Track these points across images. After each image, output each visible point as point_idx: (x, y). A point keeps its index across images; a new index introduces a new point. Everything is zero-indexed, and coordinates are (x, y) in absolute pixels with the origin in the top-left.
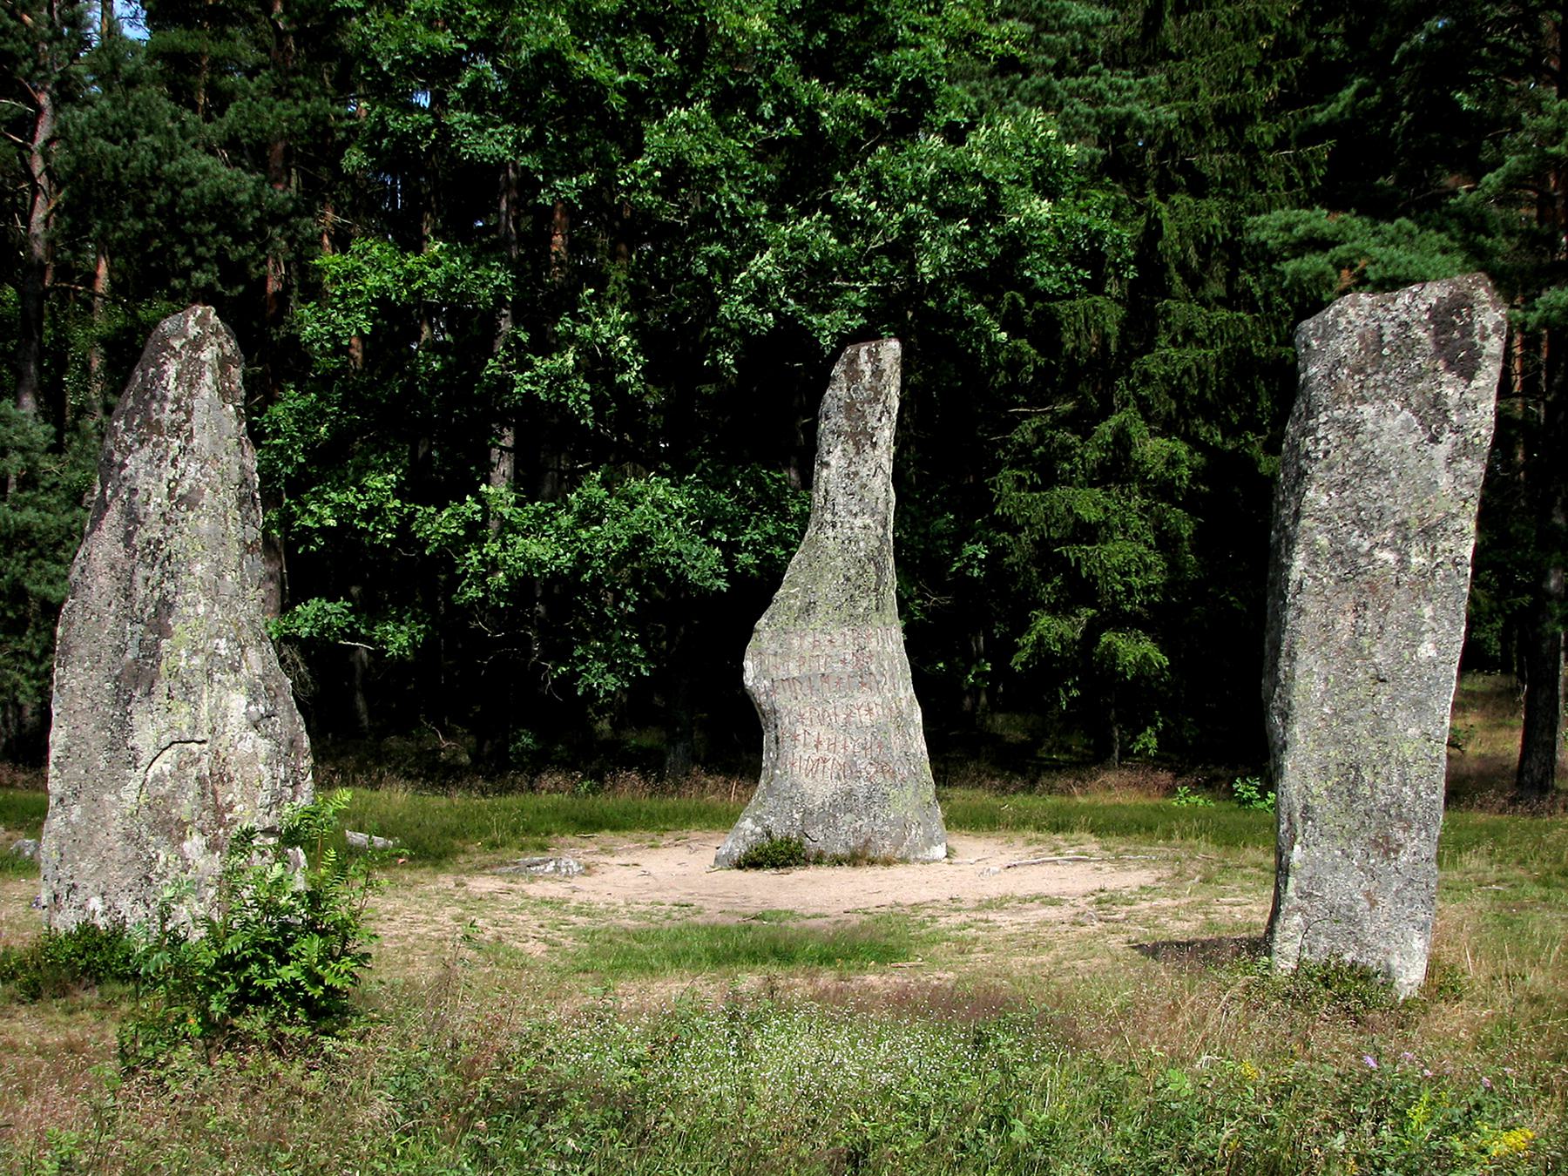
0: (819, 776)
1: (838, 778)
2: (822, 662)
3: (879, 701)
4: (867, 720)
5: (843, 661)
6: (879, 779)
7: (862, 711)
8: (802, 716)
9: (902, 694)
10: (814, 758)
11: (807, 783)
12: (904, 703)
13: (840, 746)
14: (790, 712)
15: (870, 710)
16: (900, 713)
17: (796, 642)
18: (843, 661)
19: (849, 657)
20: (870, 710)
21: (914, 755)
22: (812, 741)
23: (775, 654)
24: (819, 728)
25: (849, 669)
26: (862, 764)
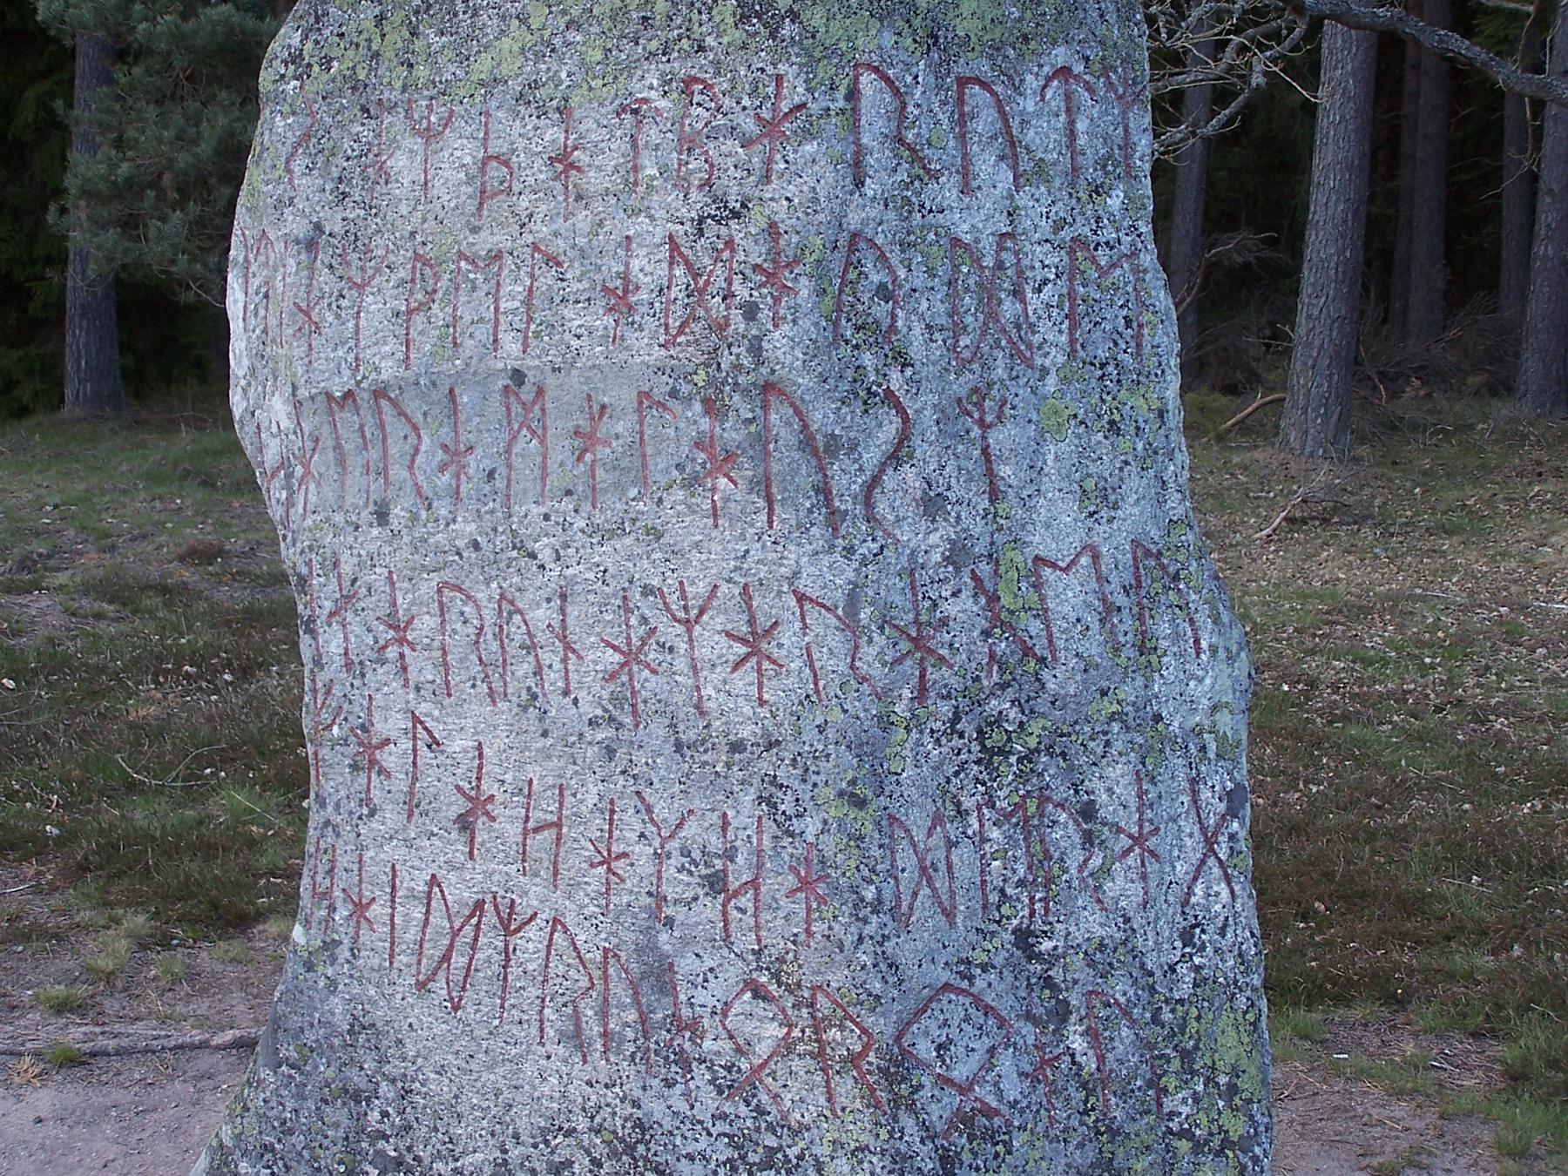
0: (479, 1004)
1: (575, 1038)
2: (513, 292)
4: (734, 702)
5: (620, 297)
6: (798, 1092)
7: (712, 642)
8: (399, 627)
9: (1055, 526)
10: (459, 892)
11: (420, 1021)
12: (1069, 596)
13: (581, 840)
14: (347, 599)
15: (755, 641)
16: (1024, 663)
17: (404, 164)
18: (620, 297)
19: (648, 268)
21: (1100, 957)
23: (311, 245)
24: (478, 710)
25: (644, 348)
26: (709, 981)
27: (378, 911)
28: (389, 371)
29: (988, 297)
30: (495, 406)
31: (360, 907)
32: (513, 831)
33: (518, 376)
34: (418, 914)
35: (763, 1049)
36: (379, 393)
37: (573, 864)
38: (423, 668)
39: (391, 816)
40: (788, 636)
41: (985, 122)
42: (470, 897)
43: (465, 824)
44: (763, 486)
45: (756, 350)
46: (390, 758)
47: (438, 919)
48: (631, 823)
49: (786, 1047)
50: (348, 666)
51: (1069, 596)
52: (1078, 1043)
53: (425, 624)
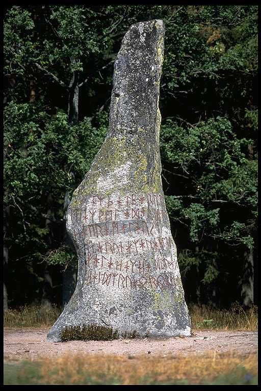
3: (149, 239)
4: (140, 250)
7: (138, 245)
10: (108, 273)
12: (165, 241)
13: (124, 266)
15: (142, 245)
20: (142, 245)
22: (106, 262)
27: (98, 277)
28: (97, 222)
29: (157, 214)
30: (111, 226)
31: (95, 277)
32: (115, 266)
33: (114, 222)
34: (103, 276)
35: (144, 283)
36: (96, 224)
37: (123, 268)
38: (104, 251)
39: (99, 267)
40: (145, 245)
41: (156, 200)
42: (110, 273)
43: (109, 266)
44: (143, 230)
45: (142, 218)
46: (99, 261)
47: (106, 276)
48: (129, 263)
49: (146, 282)
50: (93, 252)
51: (165, 241)
52: (169, 281)
53: (104, 247)
